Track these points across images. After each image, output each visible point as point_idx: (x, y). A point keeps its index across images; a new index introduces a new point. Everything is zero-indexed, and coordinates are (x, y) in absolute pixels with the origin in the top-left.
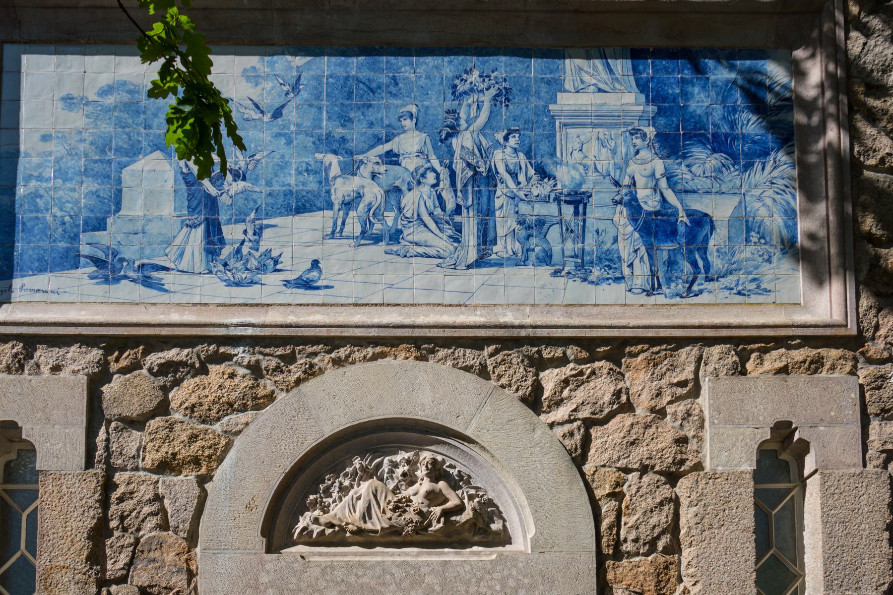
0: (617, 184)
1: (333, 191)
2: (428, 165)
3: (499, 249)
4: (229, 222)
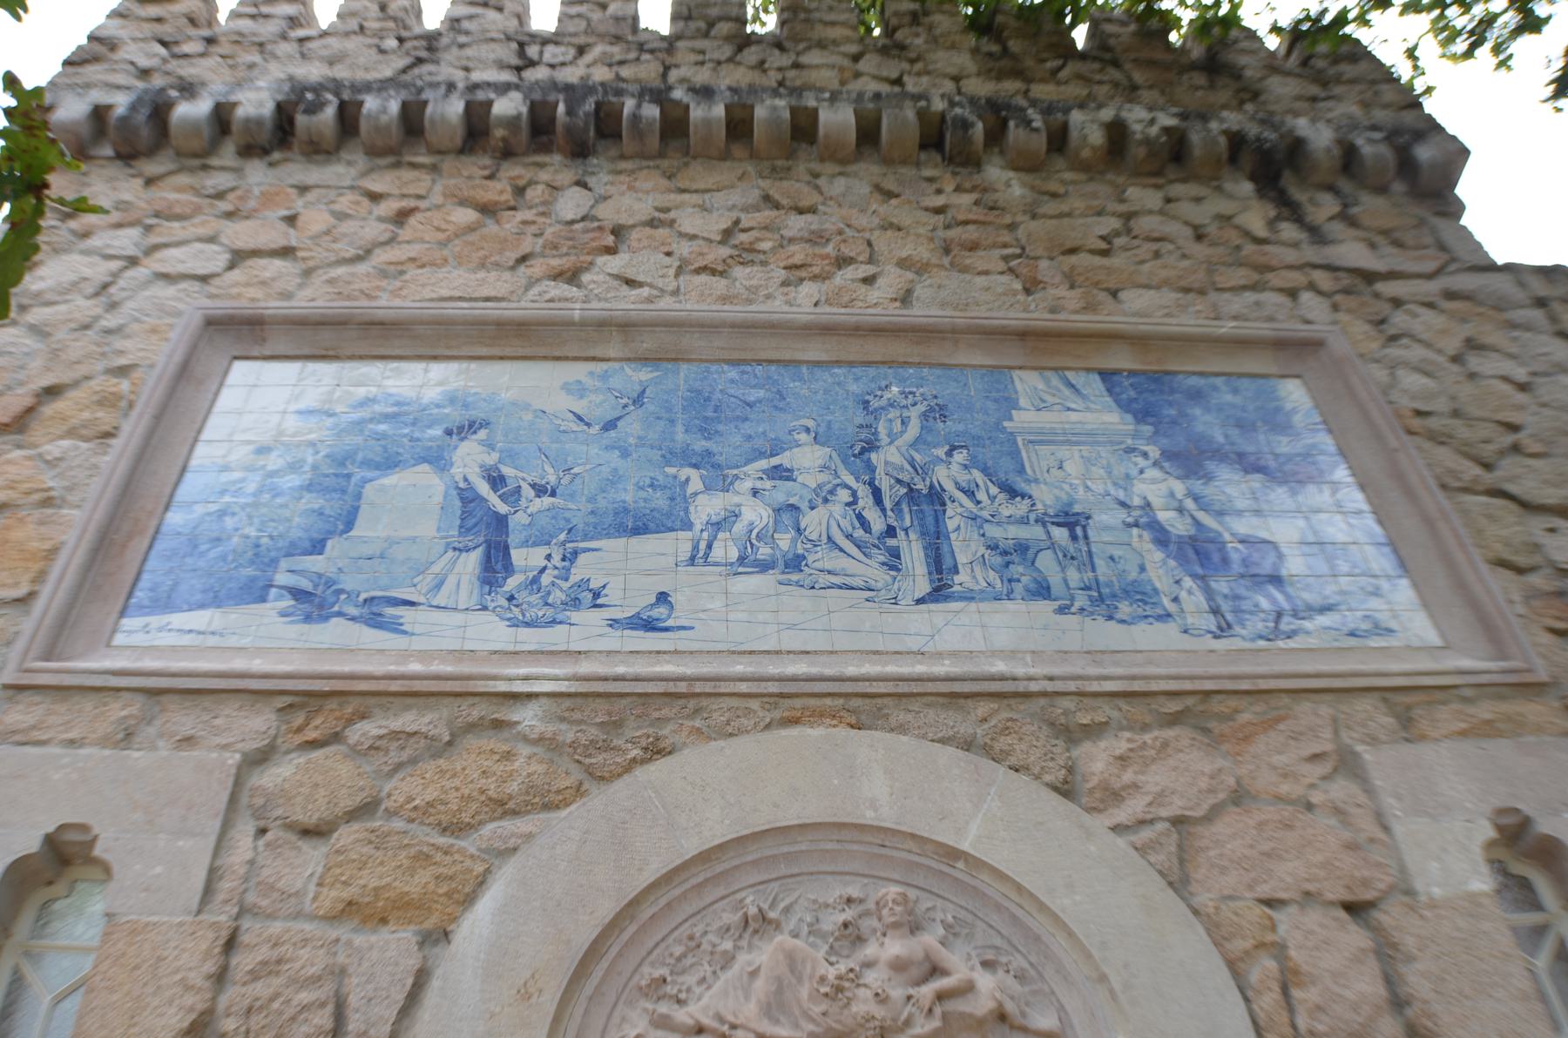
0: (1123, 504)
1: (692, 509)
2: (838, 481)
3: (963, 578)
4: (525, 544)
